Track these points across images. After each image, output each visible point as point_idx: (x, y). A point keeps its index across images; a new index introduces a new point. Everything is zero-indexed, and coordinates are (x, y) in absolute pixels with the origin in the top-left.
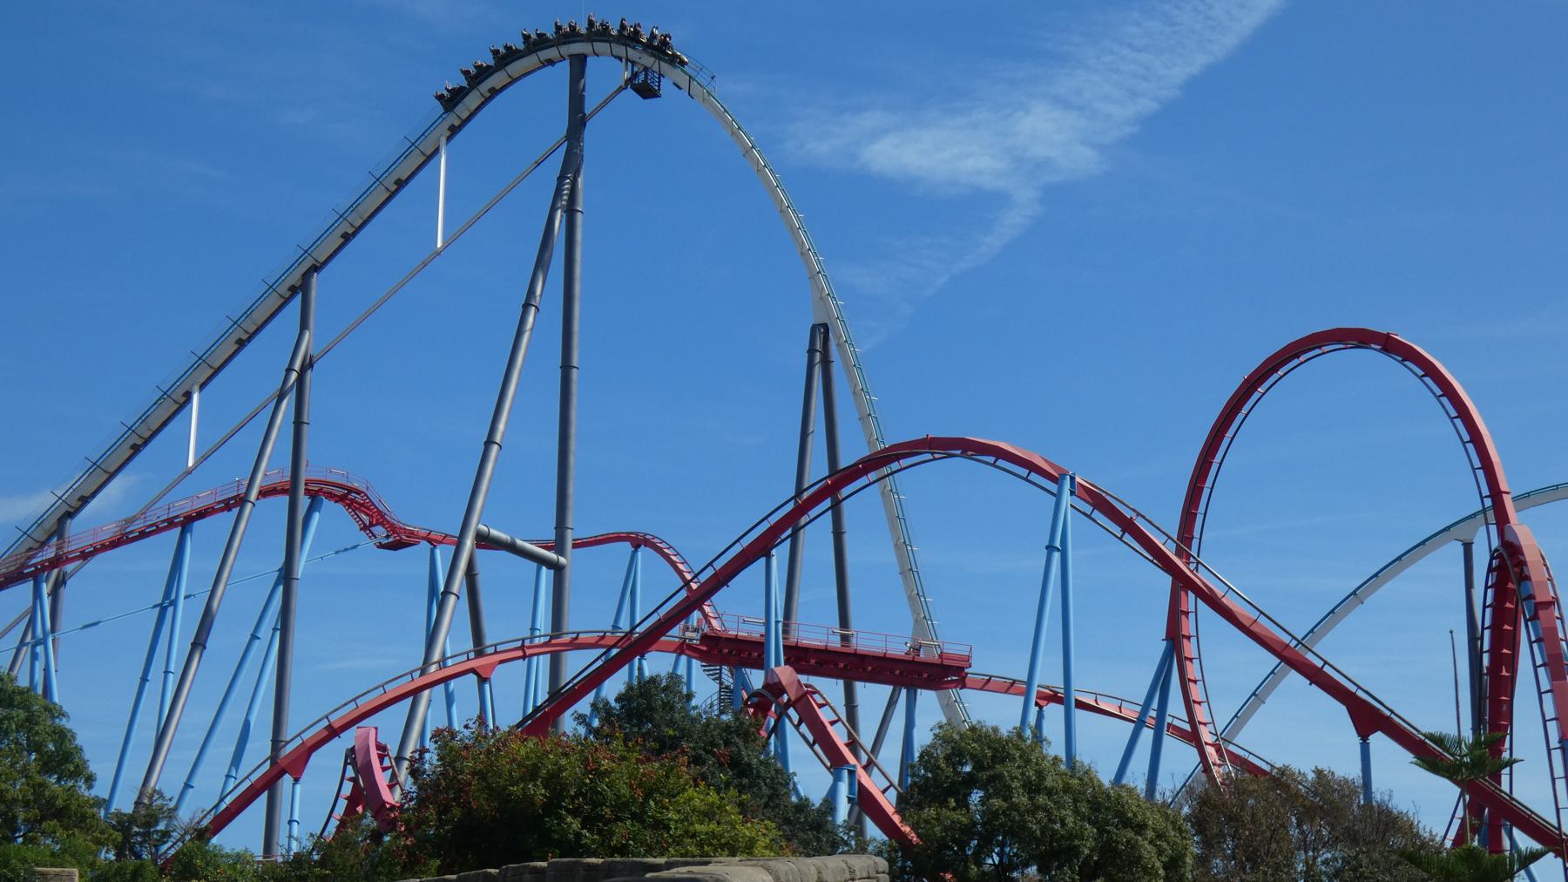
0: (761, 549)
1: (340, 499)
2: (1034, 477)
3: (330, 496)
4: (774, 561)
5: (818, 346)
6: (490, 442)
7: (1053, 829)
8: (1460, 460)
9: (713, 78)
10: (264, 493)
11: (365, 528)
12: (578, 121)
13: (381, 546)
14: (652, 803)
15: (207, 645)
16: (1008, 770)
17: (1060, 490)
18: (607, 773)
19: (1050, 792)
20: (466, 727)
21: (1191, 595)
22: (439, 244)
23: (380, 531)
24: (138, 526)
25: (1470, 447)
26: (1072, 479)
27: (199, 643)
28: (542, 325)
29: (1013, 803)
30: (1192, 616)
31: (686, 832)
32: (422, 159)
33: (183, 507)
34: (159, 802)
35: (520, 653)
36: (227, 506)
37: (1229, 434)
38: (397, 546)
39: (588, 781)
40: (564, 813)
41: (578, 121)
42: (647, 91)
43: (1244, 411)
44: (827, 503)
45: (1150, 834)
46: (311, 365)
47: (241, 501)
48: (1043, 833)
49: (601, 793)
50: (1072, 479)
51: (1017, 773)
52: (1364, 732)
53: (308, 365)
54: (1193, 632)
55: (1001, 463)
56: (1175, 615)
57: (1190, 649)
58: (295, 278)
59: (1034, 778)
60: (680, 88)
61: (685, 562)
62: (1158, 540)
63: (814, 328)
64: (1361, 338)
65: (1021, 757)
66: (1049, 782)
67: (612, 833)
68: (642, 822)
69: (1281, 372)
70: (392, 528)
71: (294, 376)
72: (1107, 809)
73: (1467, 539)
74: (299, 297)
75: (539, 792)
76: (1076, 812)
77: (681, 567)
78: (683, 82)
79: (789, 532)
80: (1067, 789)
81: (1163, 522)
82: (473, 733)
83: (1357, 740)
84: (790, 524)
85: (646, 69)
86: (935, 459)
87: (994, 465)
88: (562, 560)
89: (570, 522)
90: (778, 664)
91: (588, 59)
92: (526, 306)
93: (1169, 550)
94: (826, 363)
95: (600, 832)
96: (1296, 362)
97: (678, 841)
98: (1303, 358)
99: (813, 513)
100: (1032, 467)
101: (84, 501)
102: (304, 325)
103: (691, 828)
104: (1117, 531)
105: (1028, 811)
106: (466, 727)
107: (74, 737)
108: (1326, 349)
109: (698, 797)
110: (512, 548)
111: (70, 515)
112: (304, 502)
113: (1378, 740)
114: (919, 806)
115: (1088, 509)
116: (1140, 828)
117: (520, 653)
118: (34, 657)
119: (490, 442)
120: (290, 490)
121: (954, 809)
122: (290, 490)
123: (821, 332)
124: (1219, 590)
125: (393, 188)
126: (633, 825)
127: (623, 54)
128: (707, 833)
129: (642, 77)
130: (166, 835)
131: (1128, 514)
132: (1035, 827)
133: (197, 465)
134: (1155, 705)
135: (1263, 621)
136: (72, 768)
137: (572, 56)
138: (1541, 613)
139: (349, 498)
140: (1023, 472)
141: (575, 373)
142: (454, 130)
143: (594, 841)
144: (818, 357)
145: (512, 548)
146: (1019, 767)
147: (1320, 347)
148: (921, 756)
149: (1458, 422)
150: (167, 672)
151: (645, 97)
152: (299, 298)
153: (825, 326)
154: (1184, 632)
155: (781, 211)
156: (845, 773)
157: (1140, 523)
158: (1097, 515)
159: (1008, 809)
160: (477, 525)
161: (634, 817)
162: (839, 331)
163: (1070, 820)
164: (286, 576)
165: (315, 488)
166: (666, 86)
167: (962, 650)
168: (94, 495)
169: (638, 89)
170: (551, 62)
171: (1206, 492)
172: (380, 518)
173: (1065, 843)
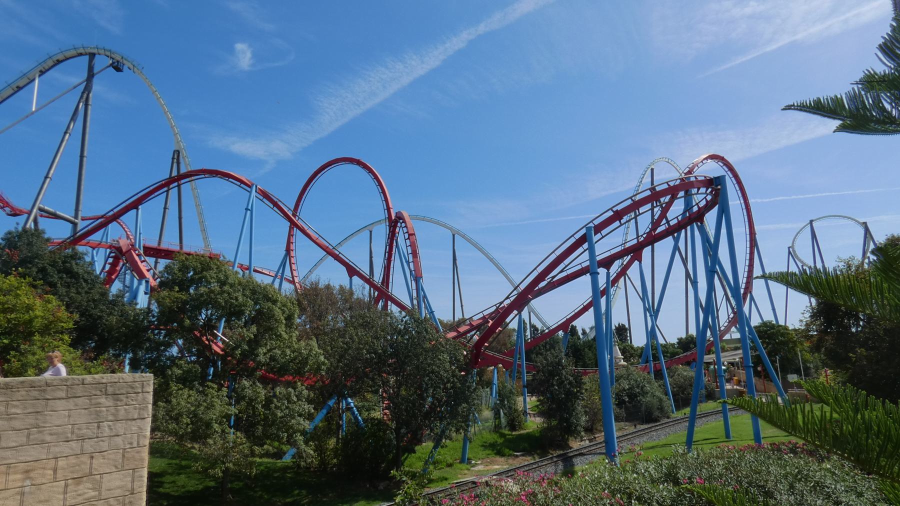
2: (242, 185)
4: (140, 211)
5: (176, 157)
6: (46, 177)
7: (231, 302)
9: (143, 68)
12: (91, 75)
13: (8, 215)
17: (251, 190)
19: (232, 286)
21: (295, 229)
22: (34, 110)
23: (8, 209)
26: (256, 186)
28: (72, 143)
30: (294, 244)
32: (28, 81)
38: (15, 215)
41: (91, 75)
42: (118, 69)
43: (314, 181)
45: (279, 304)
50: (256, 186)
51: (215, 276)
52: (351, 277)
55: (230, 180)
56: (290, 235)
57: (293, 254)
60: (130, 69)
61: (128, 228)
65: (217, 269)
66: (230, 281)
70: (12, 208)
72: (259, 293)
76: (244, 295)
77: (126, 229)
78: (131, 67)
80: (240, 284)
81: (288, 203)
83: (349, 278)
85: (118, 62)
86: (205, 178)
87: (227, 180)
89: (81, 207)
91: (97, 56)
92: (66, 133)
93: (290, 214)
94: (178, 163)
96: (330, 167)
105: (219, 294)
110: (55, 216)
113: (355, 278)
116: (275, 302)
121: (178, 292)
123: (177, 153)
124: (306, 228)
125: (16, 89)
131: (276, 200)
134: (281, 272)
137: (90, 53)
138: (410, 237)
142: (42, 73)
144: (175, 160)
145: (55, 216)
146: (215, 273)
151: (117, 71)
154: (291, 248)
155: (172, 127)
156: (144, 281)
157: (279, 203)
158: (264, 200)
159: (209, 292)
160: (40, 204)
162: (183, 153)
163: (240, 299)
166: (125, 68)
167: (218, 253)
169: (113, 67)
170: (81, 54)
173: (237, 309)
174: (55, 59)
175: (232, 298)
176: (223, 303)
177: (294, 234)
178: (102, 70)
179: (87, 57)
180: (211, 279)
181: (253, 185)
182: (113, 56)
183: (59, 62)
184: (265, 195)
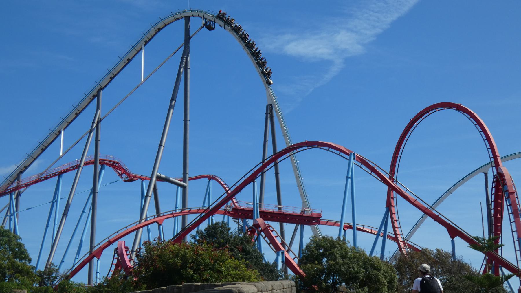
0: (251, 179)
1: (111, 165)
2: (342, 154)
3: (108, 164)
4: (256, 183)
5: (269, 112)
6: (160, 146)
7: (350, 271)
8: (483, 146)
10: (86, 164)
11: (119, 175)
12: (188, 38)
13: (125, 181)
14: (216, 264)
15: (68, 215)
16: (335, 251)
18: (201, 255)
19: (349, 259)
20: (154, 240)
21: (394, 192)
22: (142, 80)
23: (124, 176)
24: (44, 175)
25: (486, 141)
26: (354, 154)
27: (65, 214)
29: (337, 262)
30: (395, 199)
31: (228, 274)
33: (59, 169)
34: (53, 267)
35: (172, 216)
36: (74, 168)
37: (406, 138)
38: (130, 181)
39: (195, 257)
40: (187, 268)
41: (188, 38)
42: (210, 28)
43: (411, 131)
44: (273, 164)
45: (382, 272)
46: (101, 121)
47: (78, 167)
48: (347, 272)
49: (199, 262)
50: (354, 154)
51: (338, 252)
52: (452, 237)
53: (99, 121)
54: (395, 204)
55: (330, 149)
57: (394, 210)
58: (94, 92)
59: (344, 254)
60: (221, 27)
62: (383, 174)
63: (268, 106)
64: (449, 106)
67: (204, 275)
68: (213, 271)
69: (423, 118)
70: (129, 175)
71: (95, 125)
72: (368, 263)
73: (486, 172)
74: (96, 99)
75: (179, 261)
76: (358, 265)
77: (225, 186)
79: (260, 174)
80: (355, 257)
81: (385, 168)
82: (157, 242)
83: (450, 239)
84: (261, 171)
85: (210, 21)
86: (308, 149)
87: (328, 150)
88: (185, 184)
89: (188, 172)
90: (257, 218)
93: (387, 177)
94: (272, 117)
95: (199, 274)
96: (428, 114)
97: (225, 277)
98: (430, 113)
99: (268, 167)
100: (341, 151)
101: (26, 168)
102: (98, 108)
103: (230, 273)
104: (369, 171)
106: (154, 240)
107: (24, 246)
108: (438, 109)
109: (232, 262)
111: (21, 172)
112: (99, 167)
113: (457, 239)
114: (306, 264)
115: (359, 164)
116: (379, 270)
117: (172, 216)
118: (10, 220)
119: (160, 146)
120: (94, 163)
122: (94, 163)
123: (270, 107)
124: (404, 190)
125: (127, 62)
126: (210, 272)
127: (202, 16)
128: (235, 274)
129: (209, 23)
130: (55, 278)
131: (373, 166)
132: (344, 270)
133: (63, 155)
134: (383, 229)
135: (418, 200)
136: (24, 256)
137: (185, 17)
138: (511, 196)
139: (114, 165)
140: (338, 152)
141: (188, 122)
142: (147, 42)
143: (197, 278)
144: (269, 115)
147: (436, 109)
148: (306, 247)
149: (482, 133)
150: (55, 224)
152: (96, 99)
153: (271, 105)
154: (392, 205)
156: (281, 253)
157: (377, 168)
158: (363, 166)
160: (157, 173)
161: (211, 269)
162: (276, 107)
164: (94, 191)
165: (103, 162)
166: (217, 26)
167: (318, 212)
168: (29, 165)
170: (178, 19)
171: (399, 158)
172: (124, 172)
173: (354, 275)
174: (156, 28)
175: (350, 268)
176: (345, 272)
177: (394, 196)
178: (197, 32)
179: (183, 21)
180: (337, 254)
181: (351, 153)
182: (205, 16)
183: (160, 29)
184: (363, 162)
